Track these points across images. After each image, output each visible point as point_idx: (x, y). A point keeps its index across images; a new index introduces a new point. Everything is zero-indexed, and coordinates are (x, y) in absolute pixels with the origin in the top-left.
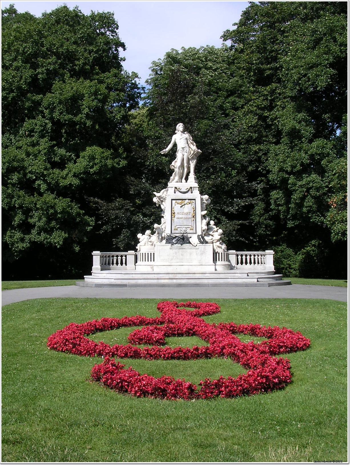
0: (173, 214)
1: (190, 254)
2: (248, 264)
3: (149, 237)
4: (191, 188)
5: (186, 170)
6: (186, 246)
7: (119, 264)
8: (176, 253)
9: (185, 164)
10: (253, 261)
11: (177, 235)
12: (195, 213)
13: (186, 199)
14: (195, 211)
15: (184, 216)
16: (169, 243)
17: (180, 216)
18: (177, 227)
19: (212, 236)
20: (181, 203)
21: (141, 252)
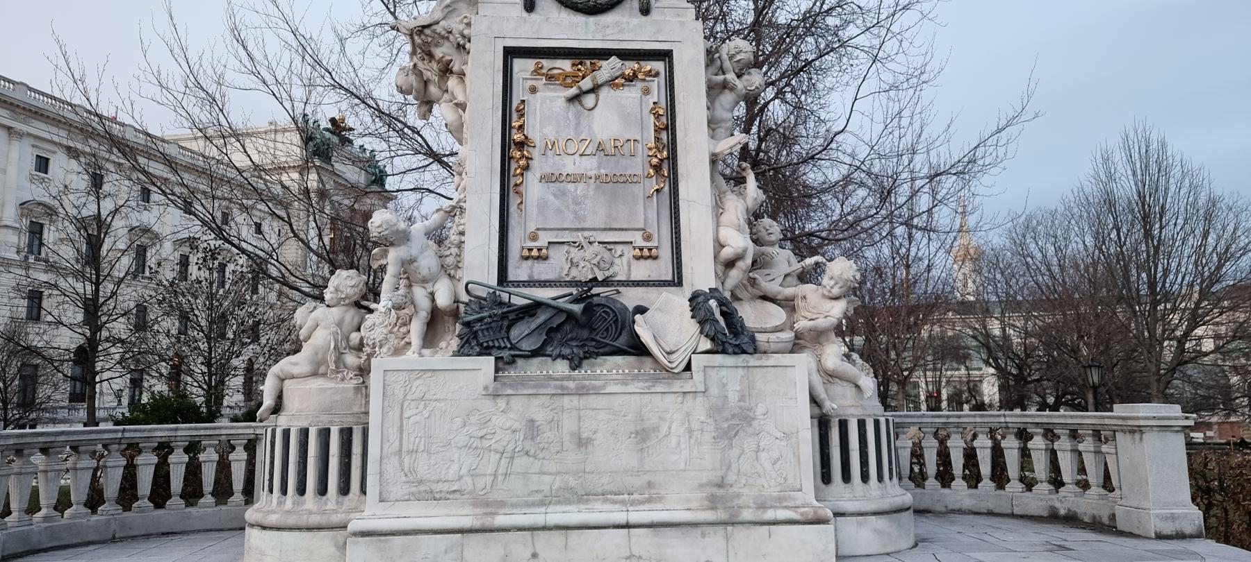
0: (513, 149)
1: (643, 435)
2: (959, 484)
3: (351, 315)
6: (612, 367)
7: (208, 499)
8: (532, 429)
10: (985, 468)
11: (545, 294)
13: (604, 54)
14: (668, 126)
15: (588, 166)
16: (485, 351)
17: (571, 165)
19: (789, 304)
20: (566, 80)
21: (282, 421)
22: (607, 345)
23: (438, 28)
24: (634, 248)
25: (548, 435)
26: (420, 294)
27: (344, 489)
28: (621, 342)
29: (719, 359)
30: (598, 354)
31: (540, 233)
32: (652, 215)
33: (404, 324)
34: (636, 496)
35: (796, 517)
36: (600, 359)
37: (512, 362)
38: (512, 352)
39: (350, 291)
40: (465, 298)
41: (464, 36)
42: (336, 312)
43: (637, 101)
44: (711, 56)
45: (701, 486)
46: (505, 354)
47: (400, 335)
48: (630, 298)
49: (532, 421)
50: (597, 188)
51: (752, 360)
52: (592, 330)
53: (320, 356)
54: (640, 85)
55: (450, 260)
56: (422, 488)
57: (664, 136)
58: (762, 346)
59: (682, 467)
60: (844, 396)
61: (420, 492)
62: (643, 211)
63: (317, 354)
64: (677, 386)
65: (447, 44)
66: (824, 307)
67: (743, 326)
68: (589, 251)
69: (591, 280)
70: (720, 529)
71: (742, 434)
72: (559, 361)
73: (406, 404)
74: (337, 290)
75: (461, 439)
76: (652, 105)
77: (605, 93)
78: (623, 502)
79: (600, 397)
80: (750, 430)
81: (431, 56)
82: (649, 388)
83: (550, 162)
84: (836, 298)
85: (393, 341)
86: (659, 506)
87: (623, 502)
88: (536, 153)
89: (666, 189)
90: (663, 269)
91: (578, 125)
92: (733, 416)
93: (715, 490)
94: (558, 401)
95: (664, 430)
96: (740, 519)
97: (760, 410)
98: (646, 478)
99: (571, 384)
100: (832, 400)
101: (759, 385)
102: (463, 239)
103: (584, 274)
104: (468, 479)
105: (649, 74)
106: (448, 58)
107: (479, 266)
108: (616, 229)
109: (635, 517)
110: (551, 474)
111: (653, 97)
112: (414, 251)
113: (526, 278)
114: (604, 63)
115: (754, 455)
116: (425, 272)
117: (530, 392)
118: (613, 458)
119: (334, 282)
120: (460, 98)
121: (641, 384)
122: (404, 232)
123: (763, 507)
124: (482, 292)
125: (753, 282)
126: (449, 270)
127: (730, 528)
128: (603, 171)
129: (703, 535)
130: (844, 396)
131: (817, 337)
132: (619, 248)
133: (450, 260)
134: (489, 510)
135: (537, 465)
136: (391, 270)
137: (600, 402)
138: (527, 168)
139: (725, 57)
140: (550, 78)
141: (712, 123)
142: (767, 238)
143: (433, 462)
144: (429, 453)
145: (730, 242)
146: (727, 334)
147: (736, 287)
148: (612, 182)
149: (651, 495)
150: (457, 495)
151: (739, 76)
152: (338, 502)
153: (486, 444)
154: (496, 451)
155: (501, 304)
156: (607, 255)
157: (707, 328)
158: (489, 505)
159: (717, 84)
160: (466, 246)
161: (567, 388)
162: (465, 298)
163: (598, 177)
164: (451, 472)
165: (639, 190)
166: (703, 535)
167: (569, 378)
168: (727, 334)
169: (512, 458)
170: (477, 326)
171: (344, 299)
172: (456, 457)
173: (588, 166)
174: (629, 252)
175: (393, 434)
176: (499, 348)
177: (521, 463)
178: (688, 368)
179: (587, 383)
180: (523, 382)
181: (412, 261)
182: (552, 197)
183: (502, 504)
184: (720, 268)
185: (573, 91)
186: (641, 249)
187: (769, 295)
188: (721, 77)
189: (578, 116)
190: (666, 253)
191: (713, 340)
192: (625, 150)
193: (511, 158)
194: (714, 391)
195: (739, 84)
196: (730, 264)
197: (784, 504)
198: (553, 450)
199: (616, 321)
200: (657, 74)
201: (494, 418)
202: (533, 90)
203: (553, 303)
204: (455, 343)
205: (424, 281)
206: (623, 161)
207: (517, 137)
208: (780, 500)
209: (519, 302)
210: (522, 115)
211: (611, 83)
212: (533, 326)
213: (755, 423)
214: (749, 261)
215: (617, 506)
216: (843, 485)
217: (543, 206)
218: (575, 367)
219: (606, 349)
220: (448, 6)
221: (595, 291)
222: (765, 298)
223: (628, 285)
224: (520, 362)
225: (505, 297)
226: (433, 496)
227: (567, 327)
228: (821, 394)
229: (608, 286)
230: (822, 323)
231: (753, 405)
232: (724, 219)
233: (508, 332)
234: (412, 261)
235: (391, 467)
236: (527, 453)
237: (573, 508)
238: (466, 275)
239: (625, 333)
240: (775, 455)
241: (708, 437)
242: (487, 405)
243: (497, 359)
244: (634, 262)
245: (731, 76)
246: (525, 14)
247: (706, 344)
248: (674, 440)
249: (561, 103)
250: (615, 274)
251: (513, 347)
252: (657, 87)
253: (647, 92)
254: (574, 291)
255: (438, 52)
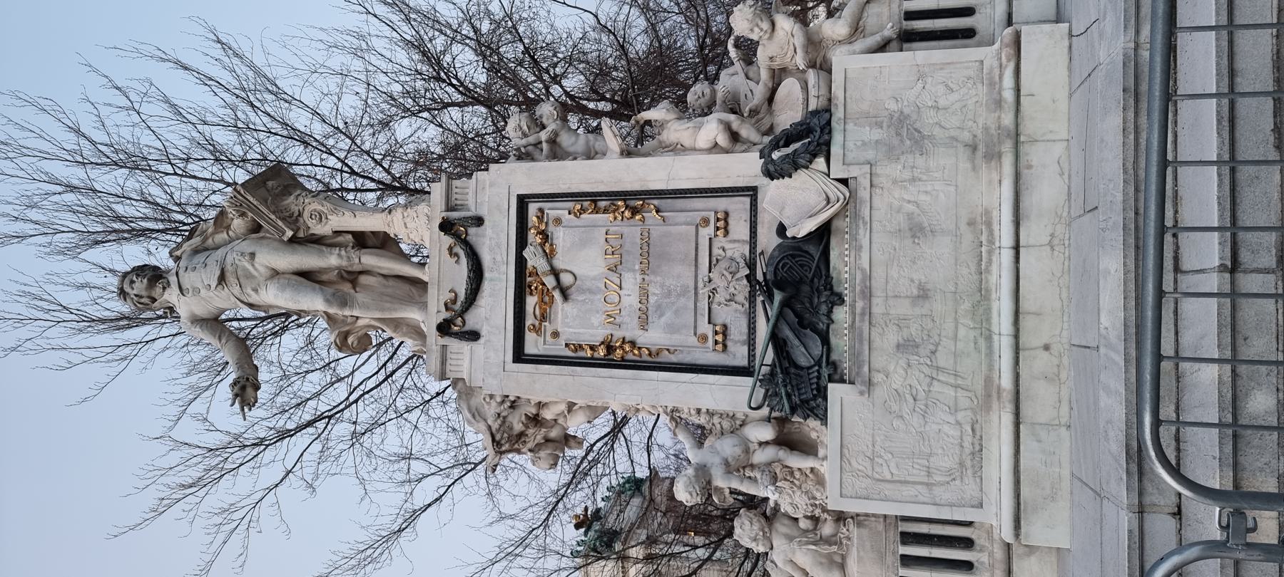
0: (613, 357)
1: (917, 230)
3: (781, 527)
4: (446, 226)
5: (370, 260)
6: (843, 262)
8: (906, 346)
9: (332, 260)
12: (613, 195)
13: (521, 263)
14: (592, 200)
15: (631, 281)
16: (822, 393)
17: (631, 299)
18: (705, 328)
19: (778, 75)
22: (818, 266)
23: (495, 426)
24: (716, 236)
25: (914, 330)
26: (760, 457)
27: (967, 543)
28: (815, 251)
29: (835, 149)
30: (828, 275)
31: (699, 332)
32: (682, 219)
33: (792, 473)
34: (984, 238)
35: (1012, 66)
36: (833, 273)
37: (834, 365)
38: (824, 364)
39: (756, 527)
40: (765, 411)
41: (503, 402)
42: (777, 542)
43: (568, 231)
44: (523, 156)
45: (974, 169)
46: (825, 372)
47: (803, 478)
48: (768, 241)
49: (898, 346)
50: (654, 273)
51: (838, 114)
52: (801, 281)
53: (824, 560)
54: (551, 228)
55: (726, 424)
56: (968, 463)
57: (602, 204)
58: (823, 102)
59: (952, 189)
60: (879, 15)
61: (973, 466)
62: (677, 227)
63: (821, 563)
64: (864, 194)
65: (510, 419)
66: (782, 39)
67: (800, 124)
68: (719, 282)
69: (749, 281)
70: (1023, 149)
71: (918, 125)
72: (834, 317)
73: (877, 476)
74: (755, 540)
75: (916, 421)
76: (572, 216)
77: (559, 263)
78: (990, 252)
79: (874, 274)
80: (914, 116)
81: (521, 435)
82: (865, 223)
83: (627, 319)
84: (773, 24)
85: (809, 485)
86: (995, 213)
87: (990, 252)
88: (618, 334)
89: (656, 202)
90: (738, 207)
91: (590, 291)
92: (898, 134)
93: (980, 154)
94: (877, 319)
95: (911, 207)
96: (1012, 127)
97: (893, 106)
98: (963, 227)
99: (860, 305)
100: (882, 28)
101: (865, 107)
102: (704, 410)
103: (742, 288)
104: (960, 416)
105: (540, 219)
106: (523, 418)
107: (733, 395)
108: (696, 255)
109: (1007, 239)
110: (956, 328)
111: (564, 214)
112: (717, 460)
113: (746, 348)
114: (530, 264)
115: (941, 112)
116: (738, 451)
117: (866, 347)
118: (940, 262)
119: (747, 543)
120: (563, 407)
121: (861, 231)
122: (697, 470)
123: (999, 103)
124: (760, 393)
125: (754, 112)
126: (737, 426)
127: (1022, 138)
128: (637, 267)
129: (1030, 167)
130: (879, 15)
131: (814, 44)
132: (716, 251)
133: (726, 424)
134: (995, 395)
135: (947, 343)
136: (736, 485)
137: (879, 273)
138: (633, 343)
139: (524, 142)
140: (544, 318)
141: (590, 155)
142: (707, 97)
143: (940, 451)
144: (930, 455)
145: (711, 137)
146: (810, 140)
147: (758, 130)
148: (649, 256)
149: (982, 223)
150: (977, 427)
151: (543, 127)
152: (981, 551)
153: (922, 395)
154: (930, 385)
155: (772, 374)
156: (723, 264)
157: (802, 161)
158: (990, 390)
159: (551, 150)
160: (712, 407)
161: (863, 309)
162: (765, 411)
163: (643, 272)
164: (952, 433)
165: (657, 231)
166: (1030, 167)
167: (853, 307)
168: (810, 140)
169: (938, 368)
170: (796, 399)
171: (764, 533)
172: (935, 427)
173: (631, 281)
174: (720, 241)
175: (909, 491)
176: (819, 378)
177: (943, 359)
178: (844, 182)
179: (858, 288)
180: (856, 356)
181: (726, 463)
182: (663, 319)
183: (988, 381)
184: (739, 147)
185: (557, 294)
186: (718, 229)
187: (768, 95)
188: (545, 146)
189: (582, 291)
190: (722, 203)
191: (815, 156)
192: (616, 243)
193: (623, 359)
194: (870, 154)
195: (551, 127)
196: (735, 137)
197: (997, 78)
198: (930, 325)
199: (793, 256)
200: (541, 210)
201: (894, 386)
202: (556, 334)
203: (772, 321)
204: (813, 423)
205: (747, 451)
206: (627, 247)
207: (601, 352)
208: (992, 84)
209: (770, 356)
210: (580, 346)
211: (549, 256)
212: (796, 342)
213: (906, 111)
214: (732, 117)
215: (994, 259)
216: (977, 16)
217: (671, 329)
218: (840, 300)
219: (822, 267)
220: (474, 416)
221: (760, 277)
222: (770, 100)
223: (755, 243)
224: (834, 357)
225: (765, 370)
226: (978, 452)
227: (798, 307)
228: (876, 39)
229: (755, 264)
230: (799, 40)
231: (886, 113)
232: (687, 143)
233: (802, 368)
234: (726, 463)
235: (943, 494)
236: (933, 353)
237: (995, 305)
238: (742, 409)
239: (806, 248)
240: (941, 88)
241: (920, 161)
242: (879, 392)
243: (831, 380)
244: (732, 236)
245: (544, 135)
246: (482, 340)
247: (820, 162)
248: (923, 197)
249: (568, 307)
250: (743, 256)
251: (819, 363)
252: (555, 210)
253: (558, 221)
254: (760, 299)
255: (518, 427)
